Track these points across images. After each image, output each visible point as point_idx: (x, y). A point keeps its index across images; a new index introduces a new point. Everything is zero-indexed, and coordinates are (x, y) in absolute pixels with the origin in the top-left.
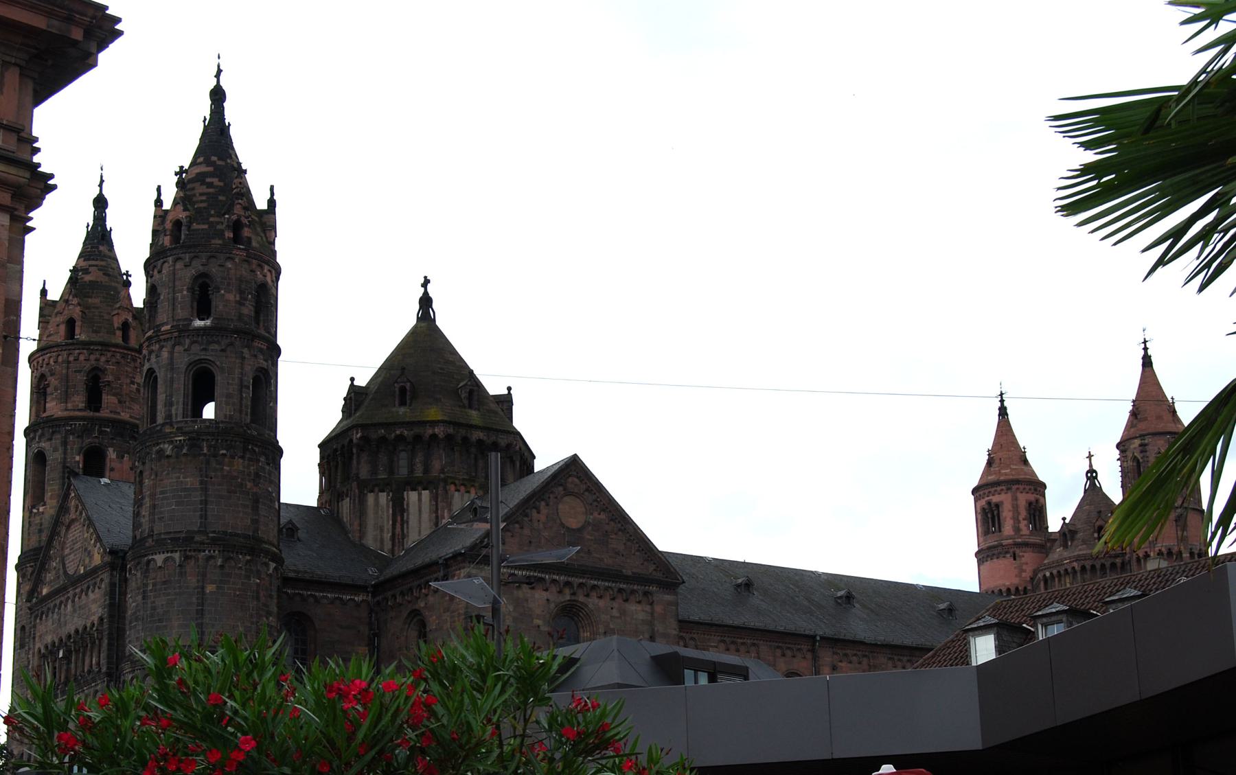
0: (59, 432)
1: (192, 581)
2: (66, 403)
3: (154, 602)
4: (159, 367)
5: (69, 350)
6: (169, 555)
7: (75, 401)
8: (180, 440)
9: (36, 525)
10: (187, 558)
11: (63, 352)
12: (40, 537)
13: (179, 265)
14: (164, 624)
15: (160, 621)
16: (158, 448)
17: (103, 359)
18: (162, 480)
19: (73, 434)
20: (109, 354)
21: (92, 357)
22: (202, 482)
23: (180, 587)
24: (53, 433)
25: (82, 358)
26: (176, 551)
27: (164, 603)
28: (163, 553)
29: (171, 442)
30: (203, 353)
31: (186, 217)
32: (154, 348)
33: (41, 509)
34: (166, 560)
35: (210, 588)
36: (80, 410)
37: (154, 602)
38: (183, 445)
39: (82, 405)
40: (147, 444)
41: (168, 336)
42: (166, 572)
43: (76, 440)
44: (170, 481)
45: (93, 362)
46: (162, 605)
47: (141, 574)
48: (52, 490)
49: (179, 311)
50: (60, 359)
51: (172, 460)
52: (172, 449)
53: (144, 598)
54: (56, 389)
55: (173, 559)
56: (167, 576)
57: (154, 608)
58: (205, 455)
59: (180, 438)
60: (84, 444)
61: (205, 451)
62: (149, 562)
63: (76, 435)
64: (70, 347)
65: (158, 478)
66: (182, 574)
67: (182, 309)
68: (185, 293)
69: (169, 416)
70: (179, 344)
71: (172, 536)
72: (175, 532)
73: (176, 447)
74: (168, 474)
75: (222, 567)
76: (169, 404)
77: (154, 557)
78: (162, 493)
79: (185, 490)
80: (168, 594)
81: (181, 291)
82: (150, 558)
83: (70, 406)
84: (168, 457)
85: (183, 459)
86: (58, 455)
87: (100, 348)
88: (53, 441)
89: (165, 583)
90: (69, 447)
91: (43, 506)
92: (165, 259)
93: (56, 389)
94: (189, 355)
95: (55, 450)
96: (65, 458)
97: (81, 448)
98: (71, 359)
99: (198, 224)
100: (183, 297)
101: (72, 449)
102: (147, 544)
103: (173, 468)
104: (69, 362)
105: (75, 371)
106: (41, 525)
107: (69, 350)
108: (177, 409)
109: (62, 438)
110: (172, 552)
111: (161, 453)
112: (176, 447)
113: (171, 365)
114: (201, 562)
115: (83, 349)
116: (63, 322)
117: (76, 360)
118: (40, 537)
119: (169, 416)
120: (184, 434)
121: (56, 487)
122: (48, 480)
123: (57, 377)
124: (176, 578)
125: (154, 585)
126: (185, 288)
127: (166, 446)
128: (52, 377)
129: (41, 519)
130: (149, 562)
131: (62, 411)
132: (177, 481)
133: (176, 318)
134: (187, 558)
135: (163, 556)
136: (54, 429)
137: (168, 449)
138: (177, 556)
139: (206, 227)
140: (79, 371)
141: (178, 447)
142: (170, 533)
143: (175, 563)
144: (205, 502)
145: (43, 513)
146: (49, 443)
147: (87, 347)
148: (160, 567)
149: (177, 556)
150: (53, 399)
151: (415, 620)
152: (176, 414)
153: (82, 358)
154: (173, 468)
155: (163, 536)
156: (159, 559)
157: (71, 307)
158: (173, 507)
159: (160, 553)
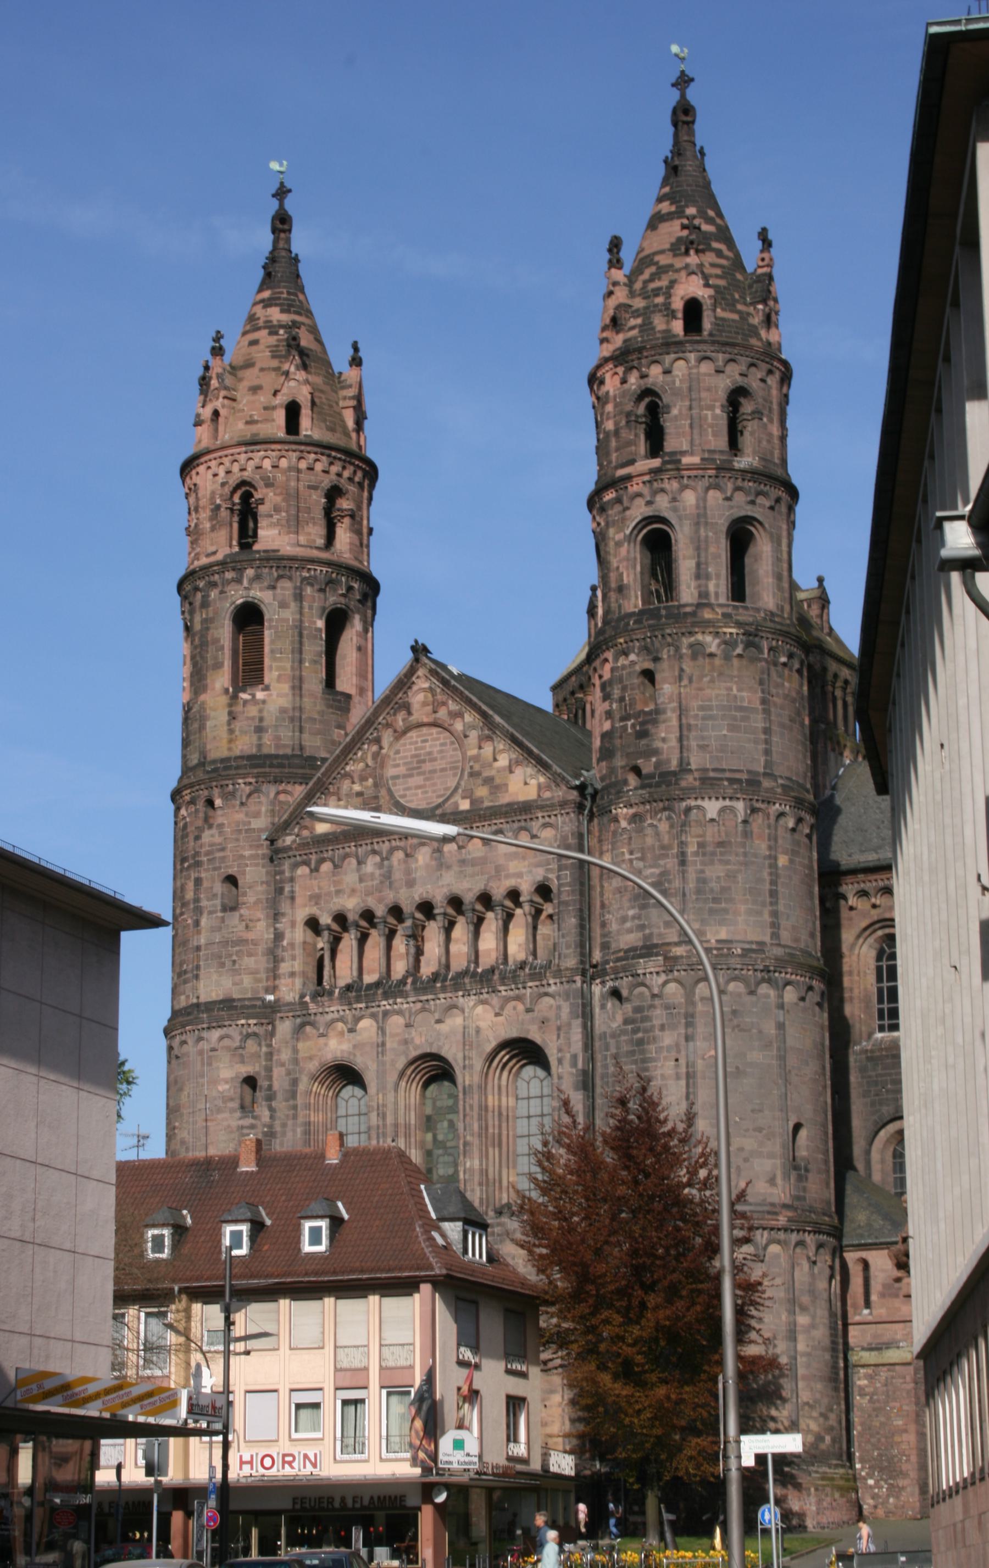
0: (290, 578)
1: (762, 847)
2: (297, 533)
3: (702, 871)
4: (680, 518)
6: (727, 803)
7: (309, 534)
9: (253, 718)
10: (754, 810)
11: (290, 453)
12: (260, 738)
13: (706, 367)
14: (723, 905)
15: (715, 900)
17: (346, 474)
18: (701, 689)
19: (312, 585)
20: (226, 461)
21: (335, 469)
22: (764, 701)
23: (745, 854)
24: (280, 577)
25: (319, 467)
27: (722, 874)
28: (724, 798)
29: (717, 634)
30: (749, 507)
31: (710, 297)
32: (666, 485)
33: (260, 695)
34: (722, 810)
35: (783, 860)
36: (317, 548)
37: (702, 871)
38: (736, 641)
39: (321, 542)
40: (668, 631)
41: (700, 472)
42: (722, 828)
43: (316, 595)
44: (717, 692)
45: (334, 477)
46: (718, 878)
47: (672, 826)
48: (278, 669)
49: (710, 437)
50: (284, 463)
51: (717, 661)
52: (719, 646)
53: (683, 863)
54: (277, 509)
55: (732, 810)
56: (723, 834)
57: (702, 881)
58: (766, 661)
60: (327, 604)
61: (766, 656)
62: (688, 810)
63: (317, 587)
64: (303, 448)
65: (694, 685)
66: (747, 834)
67: (715, 435)
68: (718, 411)
69: (704, 594)
70: (717, 487)
71: (728, 775)
72: (731, 771)
73: (725, 643)
74: (712, 681)
75: (793, 830)
76: (700, 574)
77: (699, 802)
78: (702, 708)
79: (741, 709)
80: (727, 862)
82: (693, 803)
83: (302, 539)
84: (712, 655)
85: (735, 662)
86: (289, 614)
87: (244, 449)
88: (279, 591)
89: (721, 844)
90: (305, 604)
91: (263, 690)
92: (681, 355)
93: (277, 509)
94: (731, 507)
95: (283, 605)
96: (301, 621)
97: (324, 609)
98: (303, 465)
99: (723, 310)
100: (715, 417)
101: (311, 608)
102: (683, 784)
103: (721, 674)
104: (299, 471)
105: (310, 487)
106: (261, 719)
107: (302, 451)
108: (717, 586)
109: (295, 588)
110: (731, 798)
111: (698, 651)
112: (725, 643)
113: (700, 518)
114: (772, 818)
115: (322, 454)
116: (281, 406)
117: (311, 469)
118: (260, 738)
119: (704, 594)
121: (288, 665)
122: (272, 651)
123: (278, 491)
124: (739, 840)
125: (701, 845)
126: (718, 404)
127: (709, 639)
128: (268, 490)
129: (261, 711)
130: (688, 810)
131: (293, 545)
133: (706, 447)
134: (754, 810)
136: (281, 572)
137: (712, 644)
138: (740, 806)
139: (735, 317)
140: (314, 488)
141: (729, 644)
142: (723, 770)
144: (767, 731)
145: (264, 702)
146: (270, 592)
147: (327, 452)
148: (712, 820)
149: (740, 806)
150: (272, 525)
151: (880, 933)
152: (717, 594)
153: (319, 467)
154: (721, 674)
155: (712, 774)
156: (712, 807)
157: (292, 383)
158: (725, 732)
159: (717, 798)
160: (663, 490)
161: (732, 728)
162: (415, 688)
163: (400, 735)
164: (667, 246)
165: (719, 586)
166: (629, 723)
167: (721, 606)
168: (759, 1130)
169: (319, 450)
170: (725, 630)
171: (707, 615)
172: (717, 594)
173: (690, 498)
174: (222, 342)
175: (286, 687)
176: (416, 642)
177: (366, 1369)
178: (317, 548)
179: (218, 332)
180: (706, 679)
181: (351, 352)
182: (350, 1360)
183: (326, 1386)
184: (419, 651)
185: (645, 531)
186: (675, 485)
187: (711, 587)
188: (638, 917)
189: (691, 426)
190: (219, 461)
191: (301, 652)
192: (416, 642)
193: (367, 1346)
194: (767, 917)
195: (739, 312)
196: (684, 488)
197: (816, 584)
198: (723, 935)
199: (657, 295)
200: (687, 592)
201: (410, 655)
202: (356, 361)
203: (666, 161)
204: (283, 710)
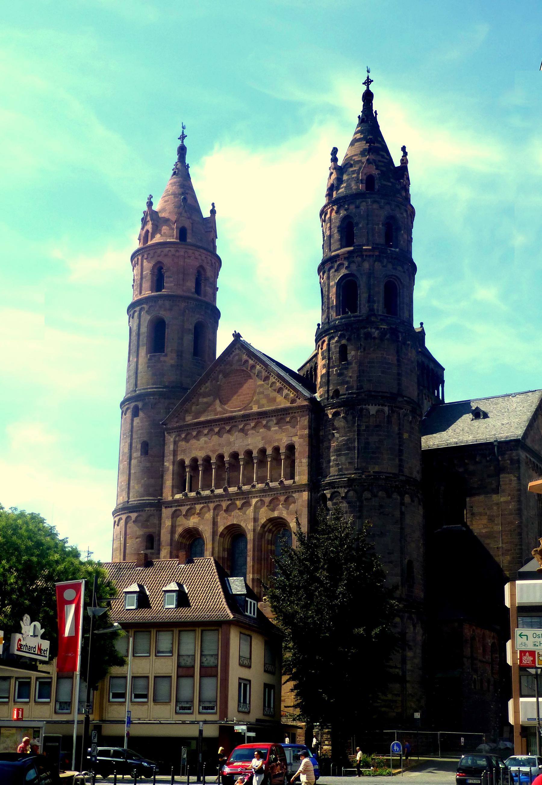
3: (367, 439)
5: (186, 249)
6: (380, 407)
8: (384, 329)
14: (377, 455)
16: (366, 330)
26: (386, 406)
28: (379, 405)
29: (377, 328)
33: (162, 359)
34: (378, 411)
35: (406, 436)
39: (194, 290)
51: (377, 341)
55: (383, 411)
59: (384, 327)
66: (389, 422)
68: (381, 226)
69: (371, 310)
70: (379, 261)
71: (381, 394)
76: (370, 300)
77: (367, 406)
81: (378, 224)
84: (375, 338)
89: (377, 426)
108: (378, 306)
111: (368, 336)
119: (371, 310)
120: (388, 324)
125: (367, 427)
126: (381, 223)
127: (373, 330)
132: (382, 357)
135: (377, 407)
137: (376, 333)
138: (386, 409)
142: (379, 392)
143: (384, 413)
155: (373, 393)
156: (373, 409)
160: (354, 262)
161: (383, 372)
162: (234, 354)
163: (226, 375)
164: (359, 152)
165: (379, 307)
166: (334, 369)
167: (381, 315)
168: (391, 562)
169: (194, 248)
170: (382, 326)
171: (373, 319)
172: (378, 310)
173: (366, 265)
174: (152, 200)
175: (174, 355)
176: (235, 331)
177: (193, 667)
178: (192, 293)
179: (151, 195)
180: (371, 349)
181: (211, 207)
182: (188, 662)
183: (173, 675)
184: (237, 336)
185: (344, 281)
186: (359, 259)
187: (375, 306)
188: (336, 460)
189: (367, 233)
190: (148, 252)
191: (182, 339)
192: (235, 331)
193: (194, 655)
194: (397, 461)
195: (392, 182)
196: (363, 260)
197: (420, 326)
198: (377, 469)
199: (354, 174)
200: (363, 309)
201: (232, 339)
202: (213, 212)
203: (359, 117)
204: (172, 366)
